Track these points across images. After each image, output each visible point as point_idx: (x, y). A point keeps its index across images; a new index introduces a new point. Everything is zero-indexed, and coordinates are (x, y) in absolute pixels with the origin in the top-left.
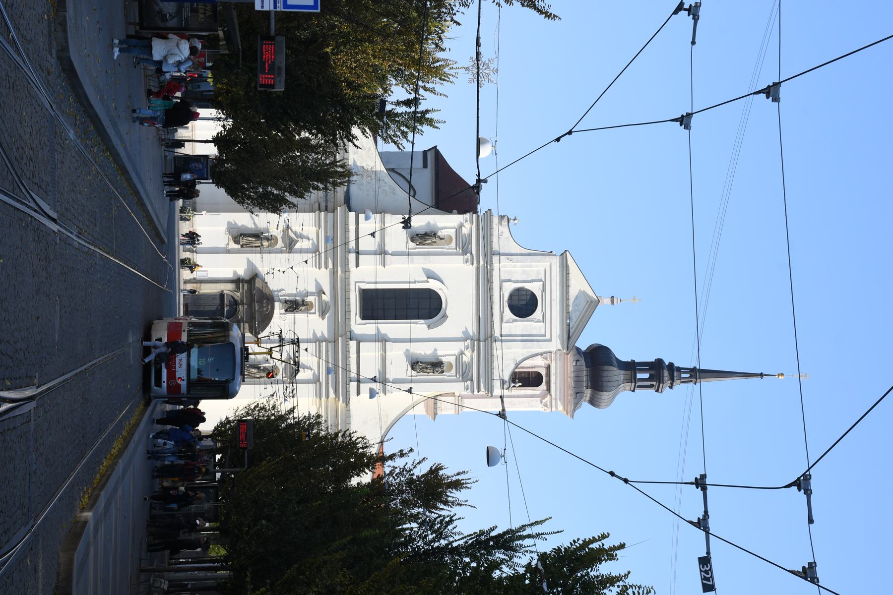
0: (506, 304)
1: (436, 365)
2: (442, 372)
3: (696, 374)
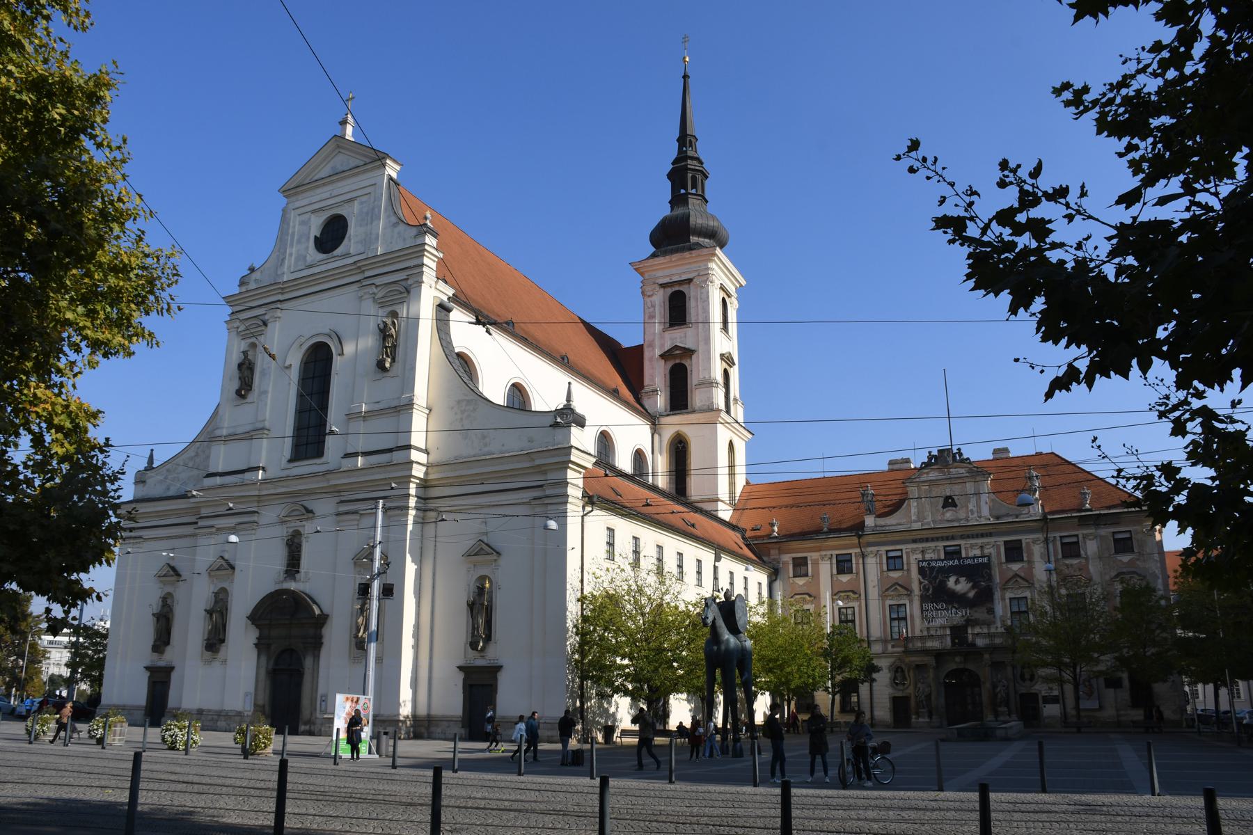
0: (330, 255)
3: (685, 139)
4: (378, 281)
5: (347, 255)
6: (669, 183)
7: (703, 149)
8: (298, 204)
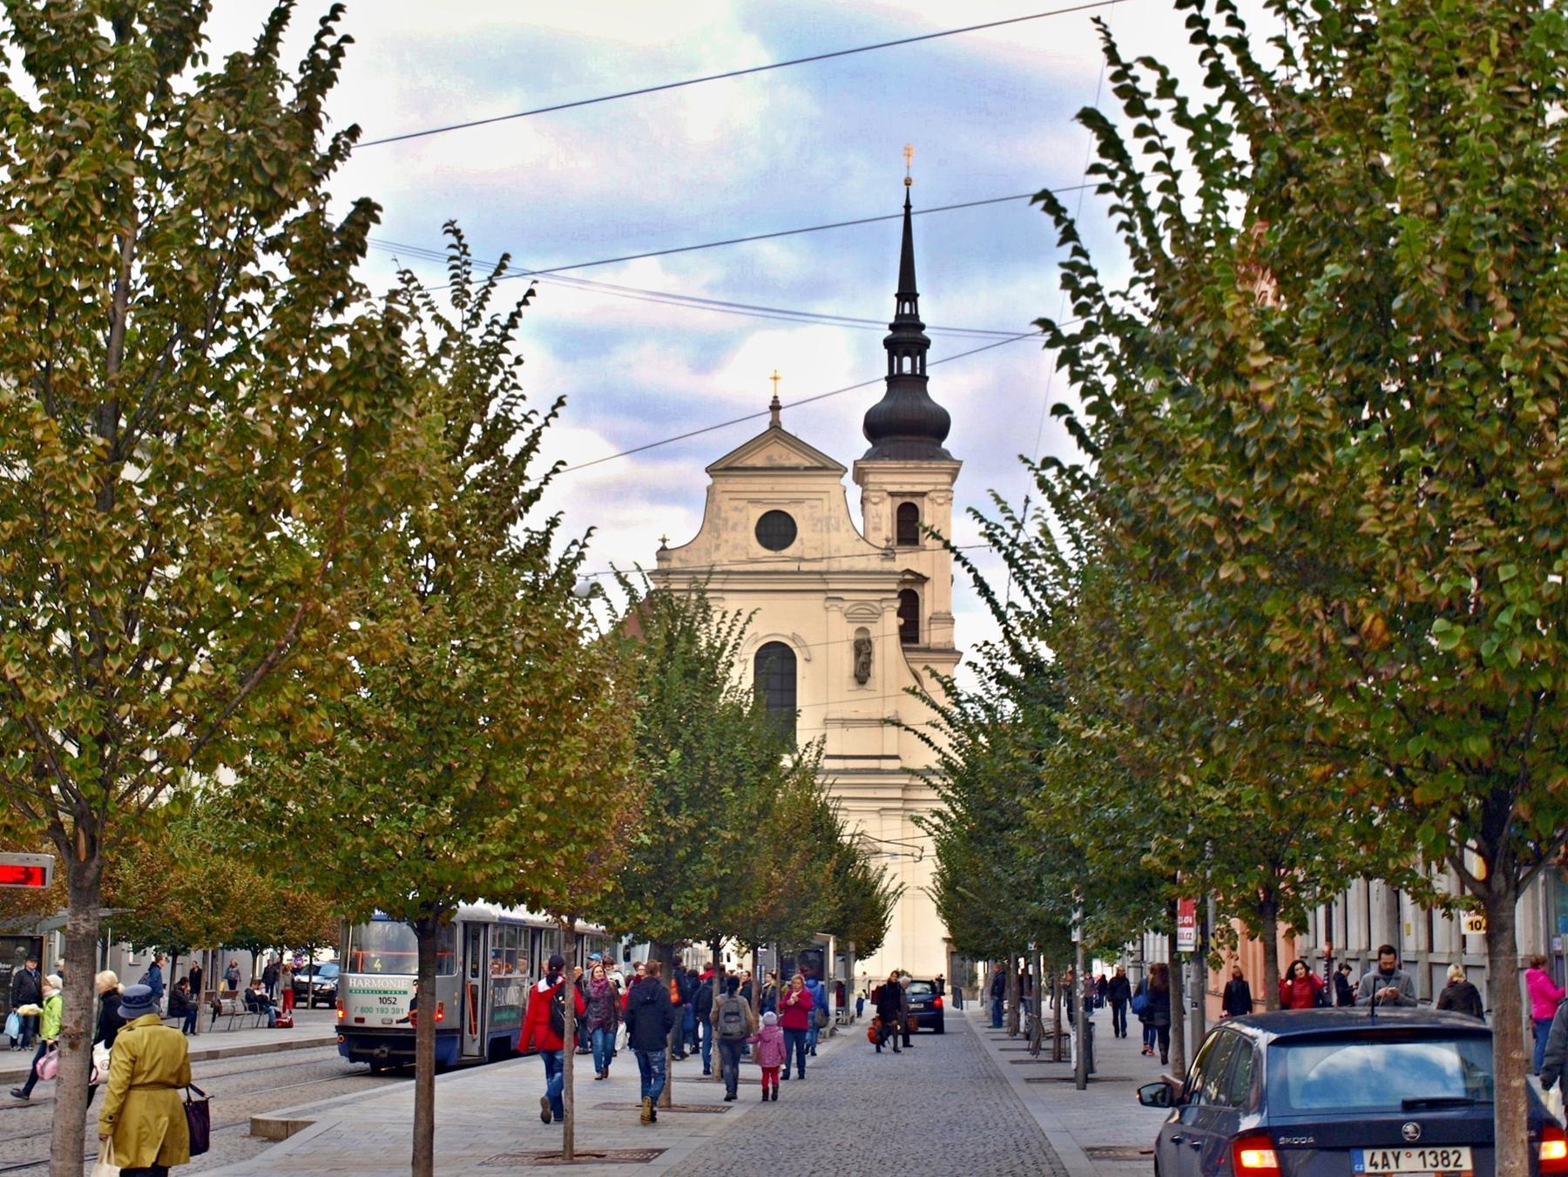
0: (779, 553)
1: (863, 650)
2: (870, 642)
4: (845, 596)
5: (802, 559)
6: (886, 352)
7: (927, 311)
8: (728, 487)
